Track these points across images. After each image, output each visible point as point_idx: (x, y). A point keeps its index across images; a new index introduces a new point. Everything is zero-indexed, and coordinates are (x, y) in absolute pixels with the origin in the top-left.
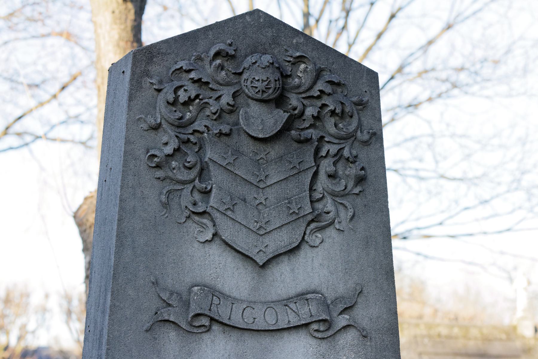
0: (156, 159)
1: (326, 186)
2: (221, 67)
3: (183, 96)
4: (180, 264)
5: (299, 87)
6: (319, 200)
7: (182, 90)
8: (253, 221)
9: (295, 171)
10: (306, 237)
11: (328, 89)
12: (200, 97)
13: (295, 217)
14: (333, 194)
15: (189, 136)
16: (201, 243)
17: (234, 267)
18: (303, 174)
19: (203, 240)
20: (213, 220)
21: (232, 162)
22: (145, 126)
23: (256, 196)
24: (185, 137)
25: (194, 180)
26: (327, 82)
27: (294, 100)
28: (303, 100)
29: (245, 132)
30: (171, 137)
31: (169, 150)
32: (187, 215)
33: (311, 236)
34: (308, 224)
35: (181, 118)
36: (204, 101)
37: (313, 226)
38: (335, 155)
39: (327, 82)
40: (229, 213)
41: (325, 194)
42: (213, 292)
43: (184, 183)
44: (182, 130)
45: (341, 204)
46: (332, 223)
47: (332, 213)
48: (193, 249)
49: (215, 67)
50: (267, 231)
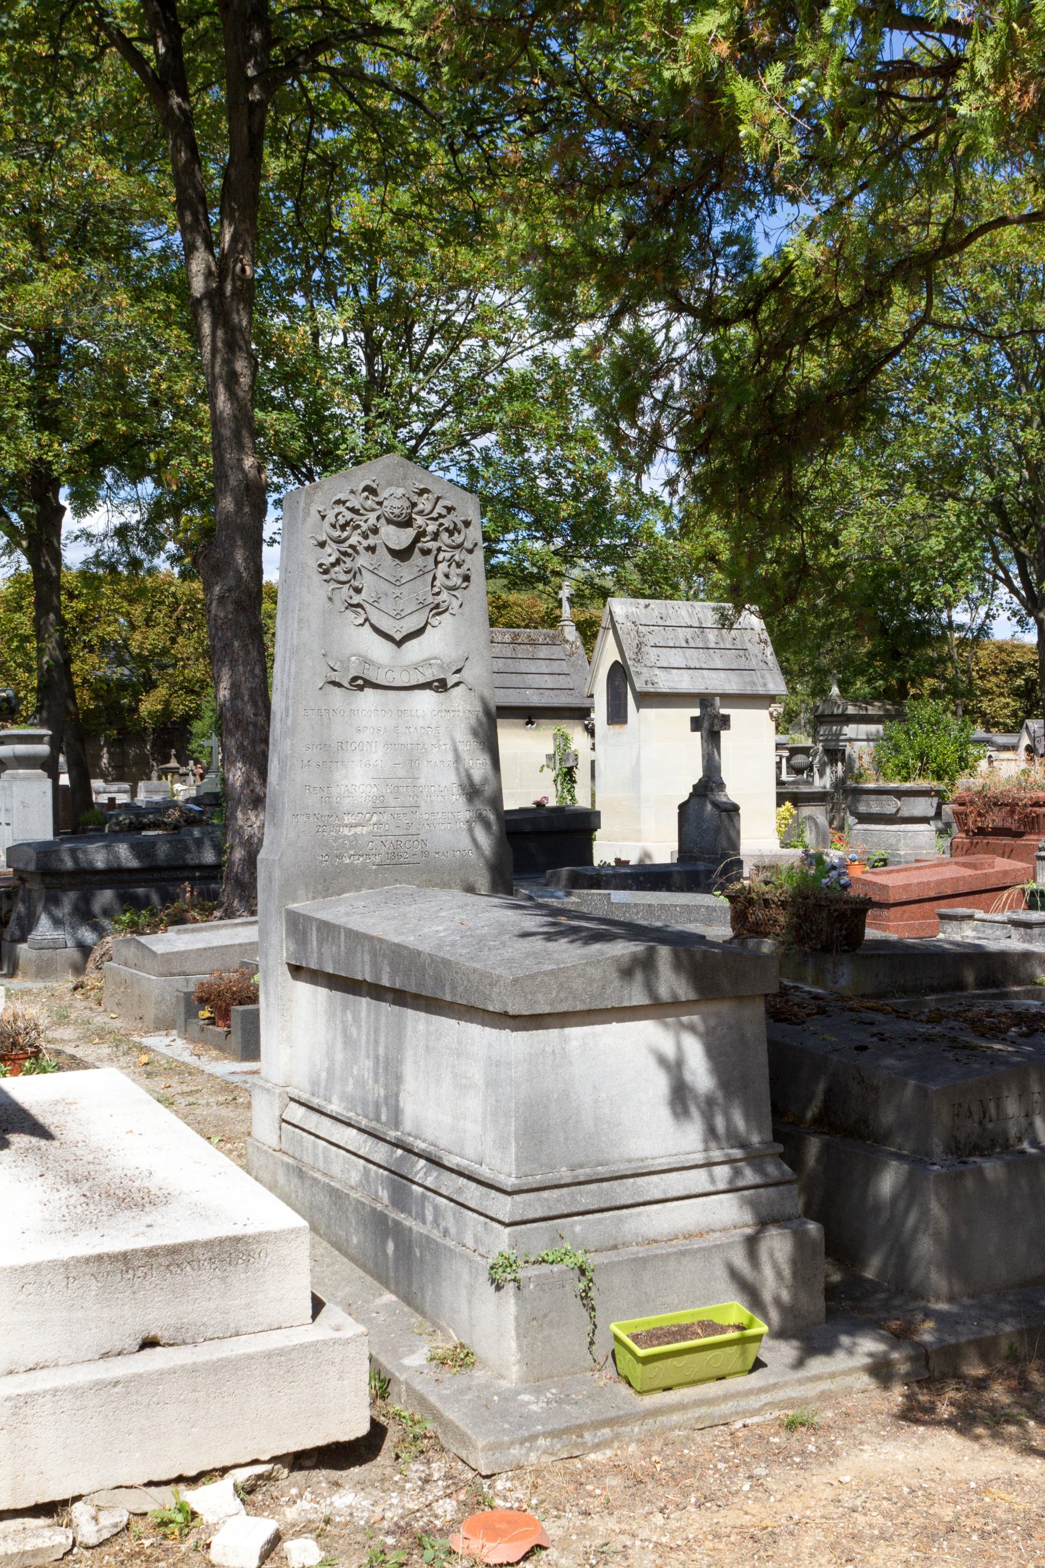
3: (342, 521)
27: (420, 520)
31: (332, 559)
42: (366, 661)
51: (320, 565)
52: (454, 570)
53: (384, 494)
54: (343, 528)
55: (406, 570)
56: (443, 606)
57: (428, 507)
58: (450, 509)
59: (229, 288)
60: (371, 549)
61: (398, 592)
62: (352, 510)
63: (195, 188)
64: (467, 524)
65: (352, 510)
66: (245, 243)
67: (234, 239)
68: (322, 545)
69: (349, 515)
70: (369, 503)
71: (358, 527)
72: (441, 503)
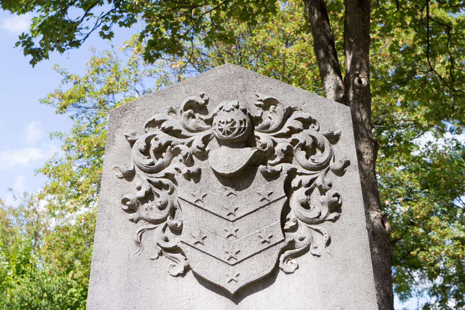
0: (128, 203)
1: (299, 215)
2: (191, 116)
4: (153, 297)
5: (268, 126)
6: (294, 229)
7: (154, 139)
8: (223, 252)
9: (265, 202)
10: (281, 265)
11: (298, 125)
12: (172, 144)
13: (266, 245)
14: (310, 222)
16: (174, 276)
17: (207, 298)
18: (272, 205)
19: (176, 274)
20: (183, 254)
21: (201, 198)
22: (120, 174)
23: (225, 228)
24: (157, 180)
25: (164, 219)
26: (296, 119)
27: (264, 138)
28: (273, 138)
29: (213, 170)
31: (141, 193)
32: (159, 251)
33: (285, 262)
34: (282, 251)
35: (153, 164)
36: (175, 147)
37: (287, 253)
39: (296, 119)
40: (198, 246)
41: (299, 221)
43: (157, 222)
45: (317, 230)
46: (306, 250)
47: (305, 239)
48: (166, 283)
50: (238, 261)
51: (124, 201)
52: (316, 198)
53: (212, 109)
54: (159, 152)
55: (246, 199)
56: (300, 245)
57: (276, 120)
58: (307, 123)
59: (351, 95)
60: (195, 176)
61: (231, 228)
62: (169, 131)
63: (326, 35)
64: (333, 138)
65: (169, 131)
66: (361, 64)
67: (353, 62)
69: (164, 138)
70: (192, 123)
71: (177, 152)
72: (295, 115)
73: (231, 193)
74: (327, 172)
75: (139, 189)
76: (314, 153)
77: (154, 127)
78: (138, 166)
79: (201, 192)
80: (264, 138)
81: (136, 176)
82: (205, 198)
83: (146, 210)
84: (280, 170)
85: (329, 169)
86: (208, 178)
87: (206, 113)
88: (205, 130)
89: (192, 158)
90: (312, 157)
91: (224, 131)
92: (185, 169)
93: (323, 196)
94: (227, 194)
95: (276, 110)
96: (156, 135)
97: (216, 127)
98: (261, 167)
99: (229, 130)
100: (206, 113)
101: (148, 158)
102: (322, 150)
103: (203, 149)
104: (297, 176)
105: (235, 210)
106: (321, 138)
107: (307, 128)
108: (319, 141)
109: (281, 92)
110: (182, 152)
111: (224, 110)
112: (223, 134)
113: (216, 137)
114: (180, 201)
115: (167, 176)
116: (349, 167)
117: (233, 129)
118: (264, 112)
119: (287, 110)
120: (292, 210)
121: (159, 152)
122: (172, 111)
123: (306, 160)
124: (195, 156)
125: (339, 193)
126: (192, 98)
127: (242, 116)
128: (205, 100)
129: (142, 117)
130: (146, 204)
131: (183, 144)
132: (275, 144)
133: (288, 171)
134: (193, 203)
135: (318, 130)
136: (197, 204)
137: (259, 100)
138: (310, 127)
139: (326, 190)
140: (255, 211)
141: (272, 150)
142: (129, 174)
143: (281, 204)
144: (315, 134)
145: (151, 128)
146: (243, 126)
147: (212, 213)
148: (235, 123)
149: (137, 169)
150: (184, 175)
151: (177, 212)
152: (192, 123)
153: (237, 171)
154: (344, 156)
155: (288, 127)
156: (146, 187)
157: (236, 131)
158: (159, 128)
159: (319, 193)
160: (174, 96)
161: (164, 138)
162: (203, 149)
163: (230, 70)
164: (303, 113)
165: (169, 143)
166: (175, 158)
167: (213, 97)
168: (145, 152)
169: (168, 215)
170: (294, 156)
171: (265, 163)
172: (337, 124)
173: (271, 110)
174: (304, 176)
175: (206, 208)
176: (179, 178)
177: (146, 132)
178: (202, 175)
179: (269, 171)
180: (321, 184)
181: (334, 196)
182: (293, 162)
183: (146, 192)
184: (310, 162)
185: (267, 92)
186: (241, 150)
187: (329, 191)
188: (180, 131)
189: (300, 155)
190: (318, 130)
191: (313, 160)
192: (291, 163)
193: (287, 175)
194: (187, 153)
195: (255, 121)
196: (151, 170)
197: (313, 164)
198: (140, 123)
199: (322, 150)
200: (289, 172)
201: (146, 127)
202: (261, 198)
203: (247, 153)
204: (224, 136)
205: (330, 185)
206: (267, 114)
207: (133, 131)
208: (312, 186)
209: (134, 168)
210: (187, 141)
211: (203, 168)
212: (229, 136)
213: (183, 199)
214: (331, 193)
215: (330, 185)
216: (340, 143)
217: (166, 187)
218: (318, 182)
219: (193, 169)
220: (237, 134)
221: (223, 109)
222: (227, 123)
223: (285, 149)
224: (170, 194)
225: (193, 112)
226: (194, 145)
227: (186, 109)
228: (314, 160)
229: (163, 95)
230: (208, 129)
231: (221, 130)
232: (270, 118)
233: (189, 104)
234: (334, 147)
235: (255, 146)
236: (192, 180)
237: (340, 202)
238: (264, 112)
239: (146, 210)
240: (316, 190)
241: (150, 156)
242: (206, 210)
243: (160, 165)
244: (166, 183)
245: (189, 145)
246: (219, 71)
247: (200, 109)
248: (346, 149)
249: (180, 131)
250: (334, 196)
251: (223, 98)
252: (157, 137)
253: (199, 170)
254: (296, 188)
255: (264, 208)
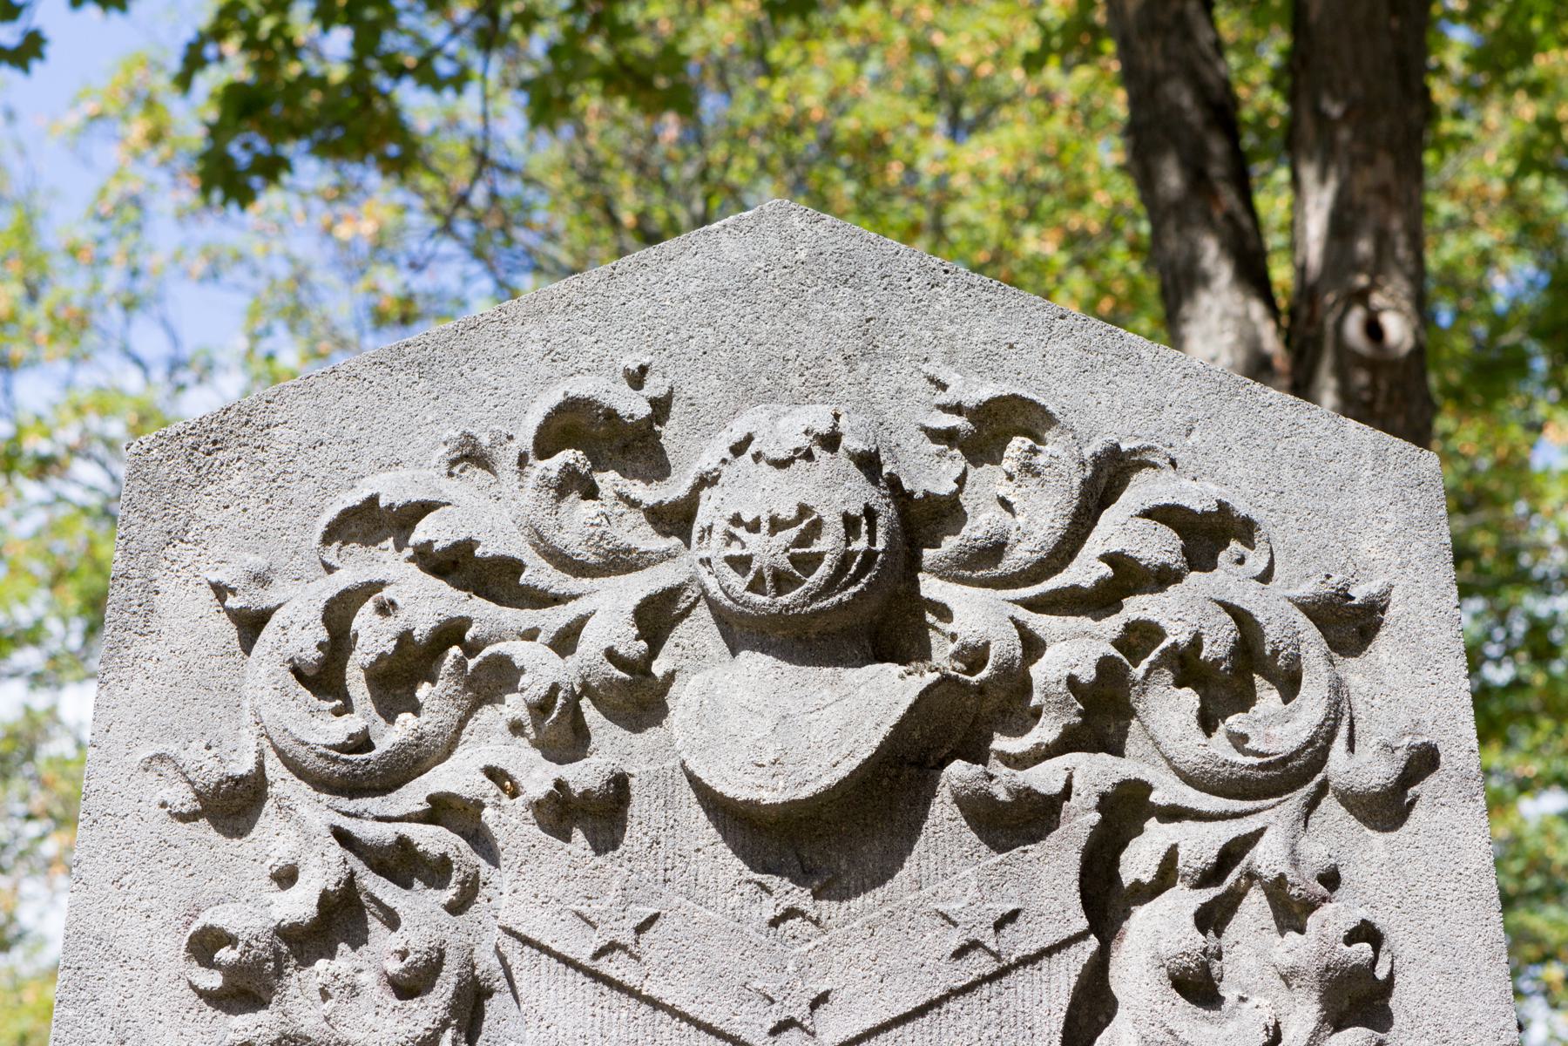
0: (226, 955)
2: (576, 485)
5: (994, 550)
7: (369, 605)
9: (980, 964)
11: (1160, 546)
12: (469, 636)
15: (408, 829)
21: (627, 938)
22: (182, 797)
24: (386, 833)
27: (973, 615)
28: (1022, 614)
29: (695, 782)
30: (309, 838)
31: (299, 904)
35: (362, 743)
36: (486, 652)
38: (1209, 877)
44: (373, 804)
49: (544, 482)
51: (205, 945)
52: (1253, 946)
53: (692, 451)
54: (398, 679)
55: (876, 947)
57: (1037, 519)
58: (1207, 534)
60: (597, 816)
64: (1349, 623)
66: (1382, 239)
67: (1341, 227)
68: (233, 806)
69: (426, 602)
70: (578, 523)
71: (496, 679)
72: (1142, 491)
73: (791, 913)
74: (1312, 804)
75: (286, 877)
76: (1245, 700)
77: (370, 538)
78: (281, 754)
79: (626, 901)
80: (973, 615)
81: (269, 806)
82: (649, 934)
83: (325, 995)
84: (1057, 787)
85: (1323, 788)
86: (668, 827)
87: (658, 468)
88: (650, 563)
89: (577, 713)
90: (1235, 722)
91: (759, 573)
92: (538, 776)
93: (1292, 936)
94: (769, 915)
95: (1041, 460)
96: (381, 585)
97: (715, 548)
98: (958, 771)
99: (784, 563)
100: (658, 468)
101: (338, 712)
102: (1289, 685)
103: (639, 668)
104: (1152, 824)
105: (814, 1005)
106: (1283, 624)
107: (1208, 565)
108: (1272, 633)
109: (1067, 366)
110: (524, 680)
111: (757, 457)
112: (752, 587)
113: (713, 605)
114: (510, 947)
115: (441, 810)
116: (1431, 780)
117: (808, 563)
118: (973, 473)
119: (1098, 461)
120: (1121, 1012)
121: (398, 679)
122: (471, 456)
123: (1200, 737)
124: (597, 703)
125: (1380, 922)
126: (582, 387)
127: (857, 493)
128: (653, 402)
129: (308, 485)
130: (321, 964)
131: (531, 635)
132: (1033, 646)
133: (1103, 797)
134: (585, 960)
135: (1266, 577)
136: (605, 966)
137: (945, 408)
138: (1222, 557)
139: (1310, 906)
140: (921, 1012)
141: (1016, 682)
142: (230, 795)
143: (1066, 972)
144: (1248, 597)
145: (354, 547)
146: (860, 544)
147: (684, 1017)
148: (816, 528)
149: (275, 769)
150: (537, 806)
151: (496, 1007)
152: (578, 523)
153: (830, 792)
154: (1403, 720)
155: (1108, 558)
156: (323, 870)
157: (824, 571)
158: (399, 548)
159: (1268, 919)
160: (481, 373)
161: (426, 602)
162: (639, 668)
163: (790, 240)
164: (1186, 483)
165: (451, 632)
166: (486, 714)
167: (697, 387)
168: (322, 678)
169: (445, 1024)
170: (1133, 713)
171: (977, 753)
172: (1367, 547)
173: (1008, 464)
174: (1188, 825)
175: (655, 992)
176: (509, 822)
177: (330, 569)
178: (635, 809)
179: (1003, 796)
180: (1284, 868)
181: (1350, 939)
182: (1131, 746)
183: (325, 896)
184: (1219, 746)
185: (986, 361)
186: (851, 675)
187: (1326, 910)
188: (516, 567)
189: (1168, 711)
190: (1266, 577)
191: (1238, 740)
192: (1117, 750)
193: (1096, 817)
194: (555, 688)
195: (923, 519)
196: (354, 776)
197: (1240, 759)
198: (294, 516)
199: (1289, 685)
200: (1106, 803)
201: (328, 537)
202: (955, 940)
203: (881, 694)
204: (758, 599)
205: (1331, 879)
206: (988, 482)
207: (258, 562)
208: (1230, 880)
209: (261, 766)
210: (554, 619)
211: (638, 769)
212: (785, 599)
213: (526, 941)
214: (1334, 918)
215: (1331, 879)
216: (1383, 648)
217: (436, 871)
218: (1267, 857)
219: (584, 775)
220: (830, 586)
221: (752, 449)
222: (776, 525)
223: (1087, 674)
224: (456, 908)
225: (584, 466)
226: (591, 644)
227: (545, 445)
228: (1244, 738)
229: (423, 368)
230: (667, 556)
231: (740, 564)
232: (1005, 504)
233: (566, 419)
234: (1354, 671)
235: (925, 654)
236: (578, 835)
237: (1381, 973)
238: (973, 473)
239: (325, 995)
240: (1255, 904)
241: (346, 697)
242: (656, 1004)
243: (403, 748)
244: (435, 850)
245: (565, 642)
246: (727, 243)
247: (626, 448)
248: (1415, 684)
249: (516, 567)
250: (1350, 939)
251: (748, 393)
252: (387, 594)
253: (620, 783)
254: (1146, 892)
255: (973, 999)
